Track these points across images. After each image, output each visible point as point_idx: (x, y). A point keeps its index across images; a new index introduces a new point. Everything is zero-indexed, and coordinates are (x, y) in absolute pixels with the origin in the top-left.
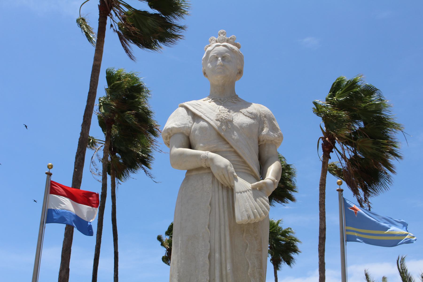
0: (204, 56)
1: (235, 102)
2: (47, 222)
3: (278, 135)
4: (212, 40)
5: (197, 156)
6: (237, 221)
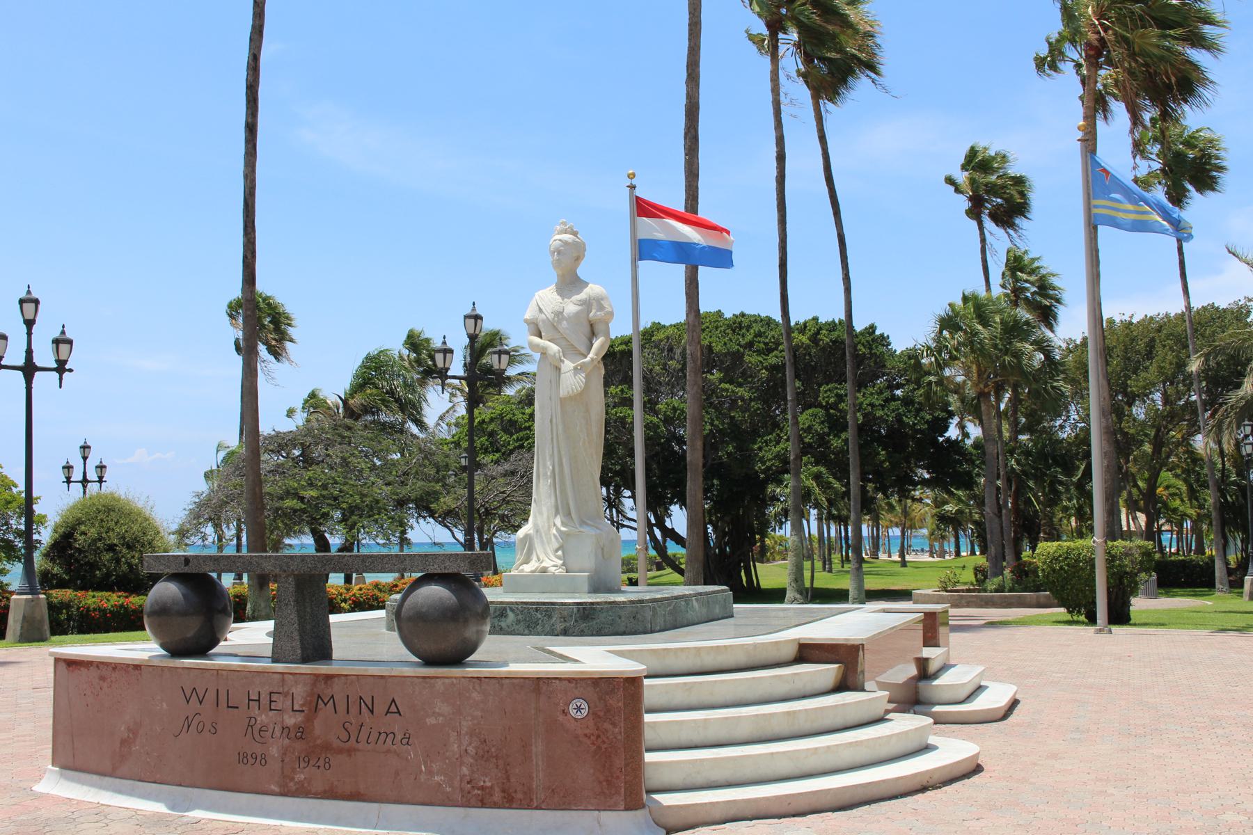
2: (641, 259)
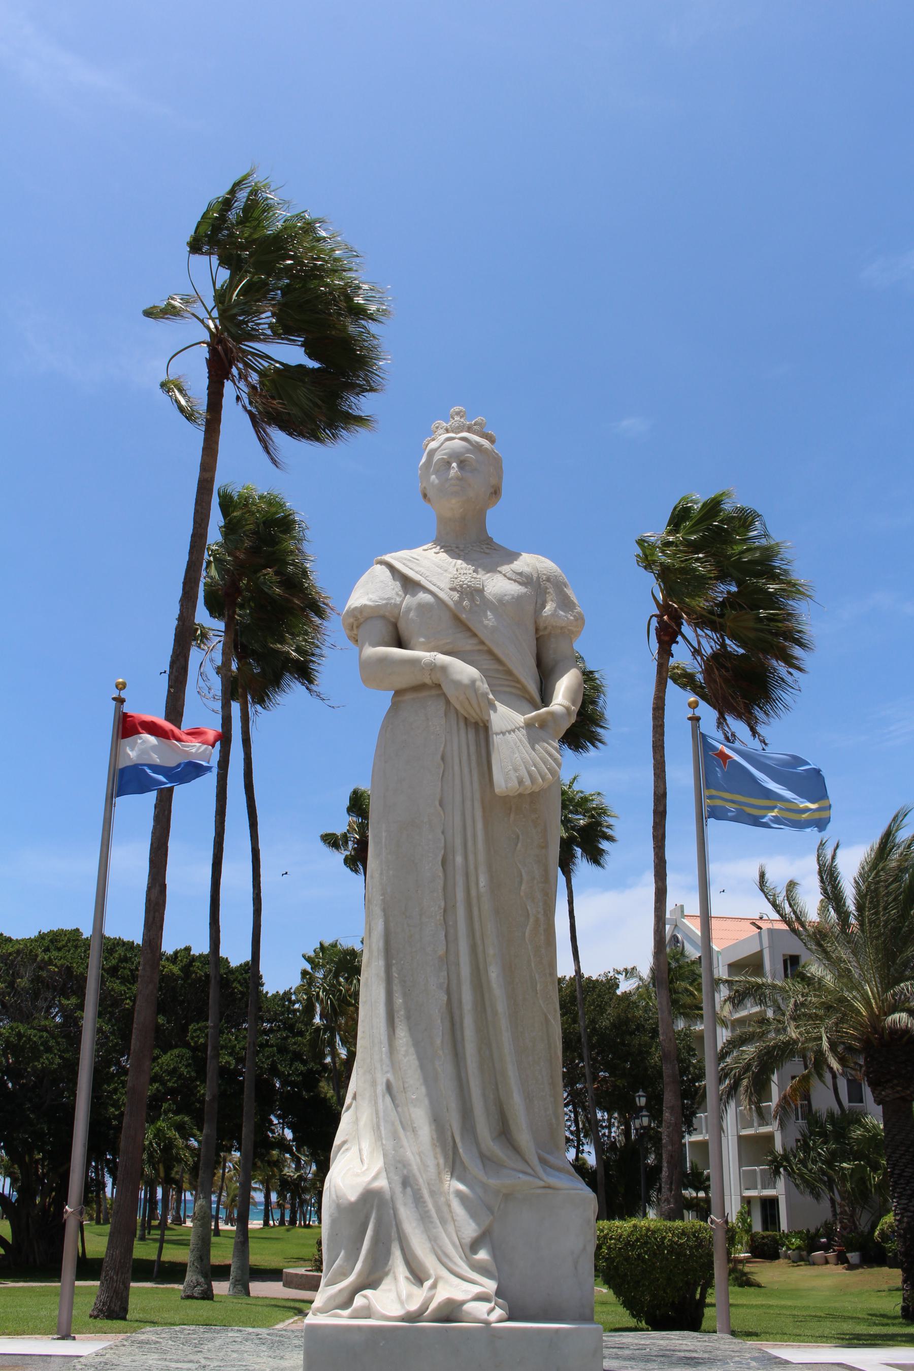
0: (423, 460)
1: (488, 551)
3: (575, 616)
4: (437, 428)
5: (415, 662)
6: (497, 790)
